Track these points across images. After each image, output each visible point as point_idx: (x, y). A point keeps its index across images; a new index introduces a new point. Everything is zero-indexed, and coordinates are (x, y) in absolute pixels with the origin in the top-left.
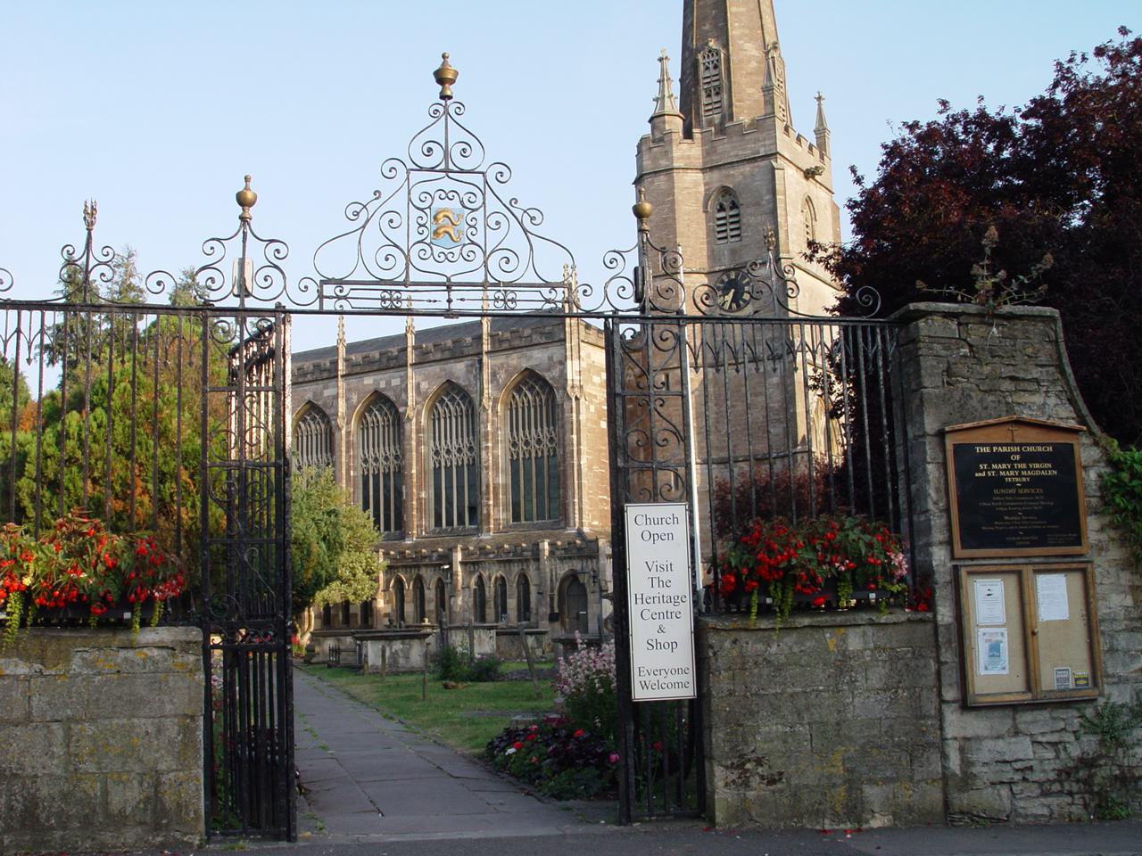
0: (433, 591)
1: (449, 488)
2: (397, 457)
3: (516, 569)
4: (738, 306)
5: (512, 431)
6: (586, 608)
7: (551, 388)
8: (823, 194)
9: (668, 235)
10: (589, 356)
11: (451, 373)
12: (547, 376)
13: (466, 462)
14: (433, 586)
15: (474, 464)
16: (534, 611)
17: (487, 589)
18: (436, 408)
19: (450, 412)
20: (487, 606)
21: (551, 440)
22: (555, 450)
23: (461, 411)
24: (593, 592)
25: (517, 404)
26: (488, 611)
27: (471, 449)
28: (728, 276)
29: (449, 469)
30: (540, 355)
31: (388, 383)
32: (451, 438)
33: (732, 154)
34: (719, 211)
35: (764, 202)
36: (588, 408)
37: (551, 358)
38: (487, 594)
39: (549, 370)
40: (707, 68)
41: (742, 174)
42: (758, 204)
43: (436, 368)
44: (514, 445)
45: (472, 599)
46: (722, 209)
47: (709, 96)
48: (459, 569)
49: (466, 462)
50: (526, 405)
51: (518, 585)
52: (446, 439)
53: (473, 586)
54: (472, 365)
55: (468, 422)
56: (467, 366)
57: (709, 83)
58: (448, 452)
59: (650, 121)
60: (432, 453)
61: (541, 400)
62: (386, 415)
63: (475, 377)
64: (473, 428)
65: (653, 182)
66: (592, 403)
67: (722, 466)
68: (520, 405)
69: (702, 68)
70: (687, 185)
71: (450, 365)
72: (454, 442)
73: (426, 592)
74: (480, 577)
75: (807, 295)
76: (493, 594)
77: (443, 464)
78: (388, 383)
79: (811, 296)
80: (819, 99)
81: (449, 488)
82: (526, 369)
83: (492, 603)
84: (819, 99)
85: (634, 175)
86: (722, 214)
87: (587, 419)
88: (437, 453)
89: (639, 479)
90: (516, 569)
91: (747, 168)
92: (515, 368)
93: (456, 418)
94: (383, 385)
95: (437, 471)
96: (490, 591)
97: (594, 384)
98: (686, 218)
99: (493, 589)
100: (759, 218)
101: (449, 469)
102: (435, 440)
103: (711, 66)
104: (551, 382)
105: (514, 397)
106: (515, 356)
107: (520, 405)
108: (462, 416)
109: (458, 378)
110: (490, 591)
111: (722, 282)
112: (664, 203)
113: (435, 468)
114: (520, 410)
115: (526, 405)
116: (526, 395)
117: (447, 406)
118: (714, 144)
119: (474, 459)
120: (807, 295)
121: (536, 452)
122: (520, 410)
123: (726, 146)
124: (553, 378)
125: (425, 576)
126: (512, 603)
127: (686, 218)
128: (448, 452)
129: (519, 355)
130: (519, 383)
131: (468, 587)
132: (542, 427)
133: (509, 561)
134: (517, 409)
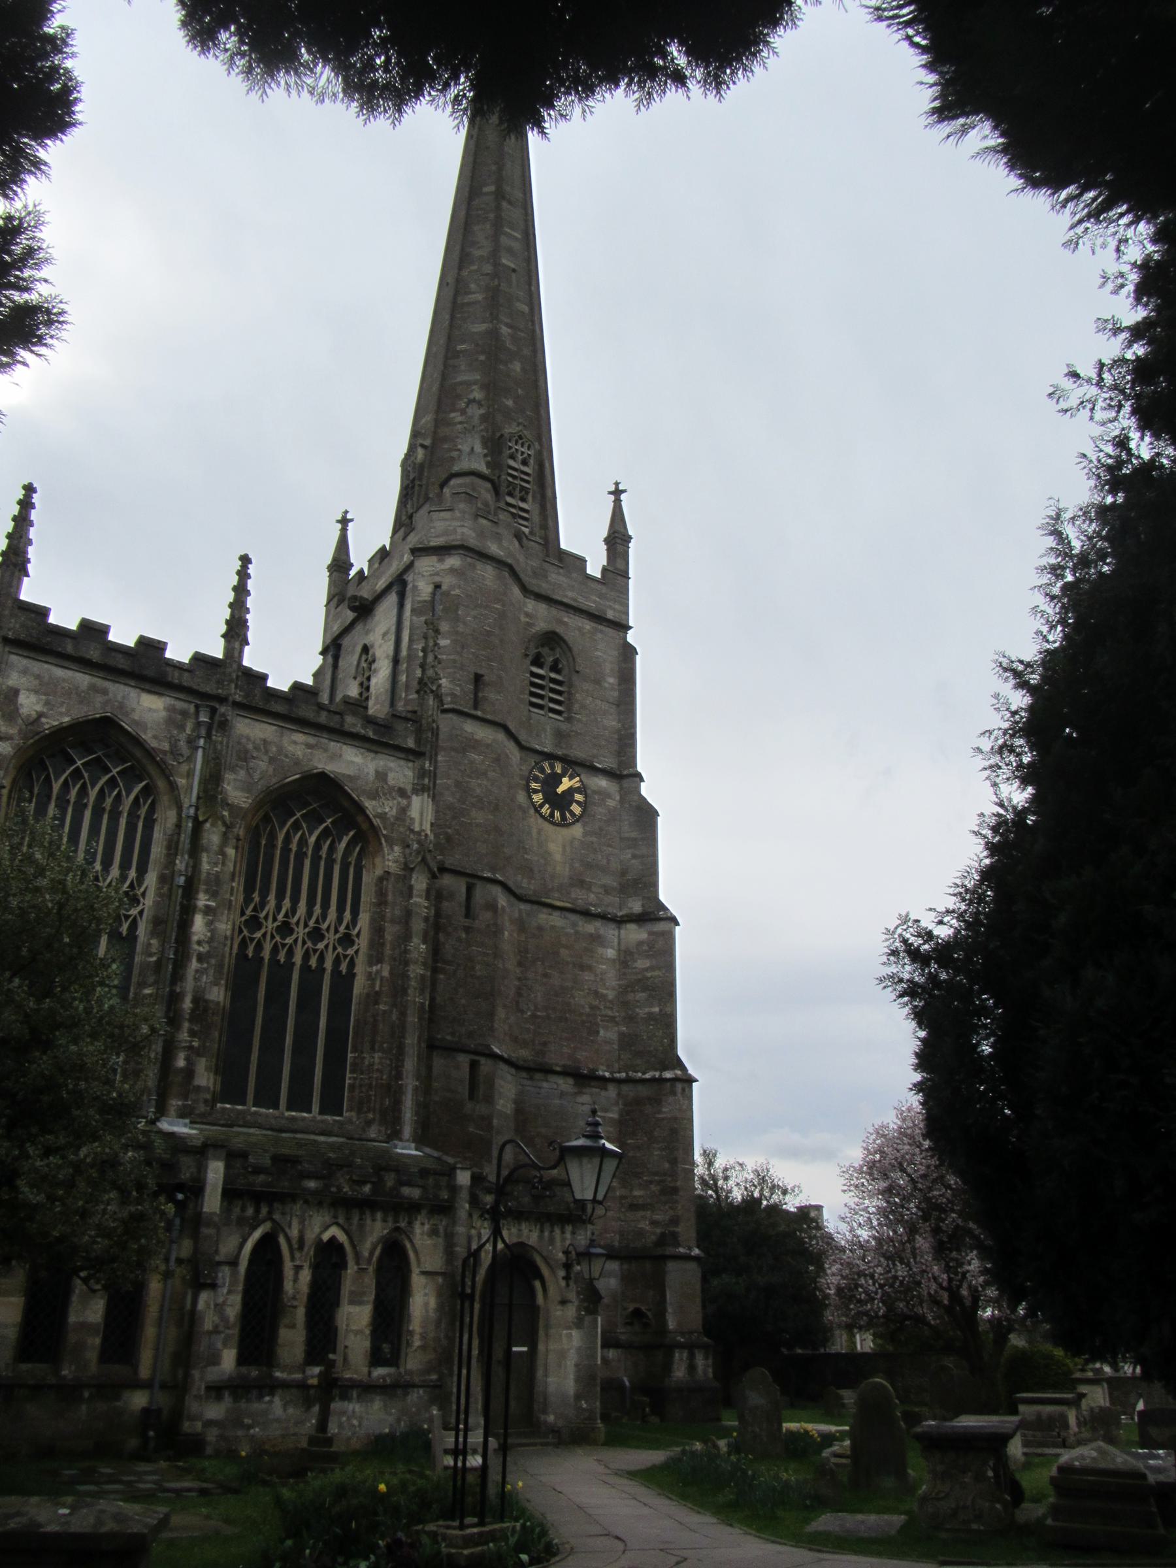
3: (377, 1229)
4: (563, 817)
12: (370, 805)
20: (285, 1321)
24: (564, 1302)
26: (284, 1334)
28: (552, 767)
33: (570, 594)
35: (606, 685)
37: (381, 776)
38: (288, 1286)
39: (374, 795)
40: (512, 457)
41: (580, 629)
42: (598, 682)
43: (83, 680)
45: (237, 1299)
46: (537, 661)
47: (510, 494)
48: (212, 1202)
51: (379, 1270)
54: (184, 713)
56: (170, 709)
57: (514, 477)
67: (524, 1074)
71: (127, 689)
82: (323, 776)
83: (301, 1313)
90: (377, 1229)
91: (588, 625)
92: (297, 763)
99: (306, 1276)
100: (599, 702)
106: (299, 737)
111: (542, 770)
118: (546, 565)
124: (382, 817)
129: (311, 740)
131: (233, 1263)
133: (366, 1205)
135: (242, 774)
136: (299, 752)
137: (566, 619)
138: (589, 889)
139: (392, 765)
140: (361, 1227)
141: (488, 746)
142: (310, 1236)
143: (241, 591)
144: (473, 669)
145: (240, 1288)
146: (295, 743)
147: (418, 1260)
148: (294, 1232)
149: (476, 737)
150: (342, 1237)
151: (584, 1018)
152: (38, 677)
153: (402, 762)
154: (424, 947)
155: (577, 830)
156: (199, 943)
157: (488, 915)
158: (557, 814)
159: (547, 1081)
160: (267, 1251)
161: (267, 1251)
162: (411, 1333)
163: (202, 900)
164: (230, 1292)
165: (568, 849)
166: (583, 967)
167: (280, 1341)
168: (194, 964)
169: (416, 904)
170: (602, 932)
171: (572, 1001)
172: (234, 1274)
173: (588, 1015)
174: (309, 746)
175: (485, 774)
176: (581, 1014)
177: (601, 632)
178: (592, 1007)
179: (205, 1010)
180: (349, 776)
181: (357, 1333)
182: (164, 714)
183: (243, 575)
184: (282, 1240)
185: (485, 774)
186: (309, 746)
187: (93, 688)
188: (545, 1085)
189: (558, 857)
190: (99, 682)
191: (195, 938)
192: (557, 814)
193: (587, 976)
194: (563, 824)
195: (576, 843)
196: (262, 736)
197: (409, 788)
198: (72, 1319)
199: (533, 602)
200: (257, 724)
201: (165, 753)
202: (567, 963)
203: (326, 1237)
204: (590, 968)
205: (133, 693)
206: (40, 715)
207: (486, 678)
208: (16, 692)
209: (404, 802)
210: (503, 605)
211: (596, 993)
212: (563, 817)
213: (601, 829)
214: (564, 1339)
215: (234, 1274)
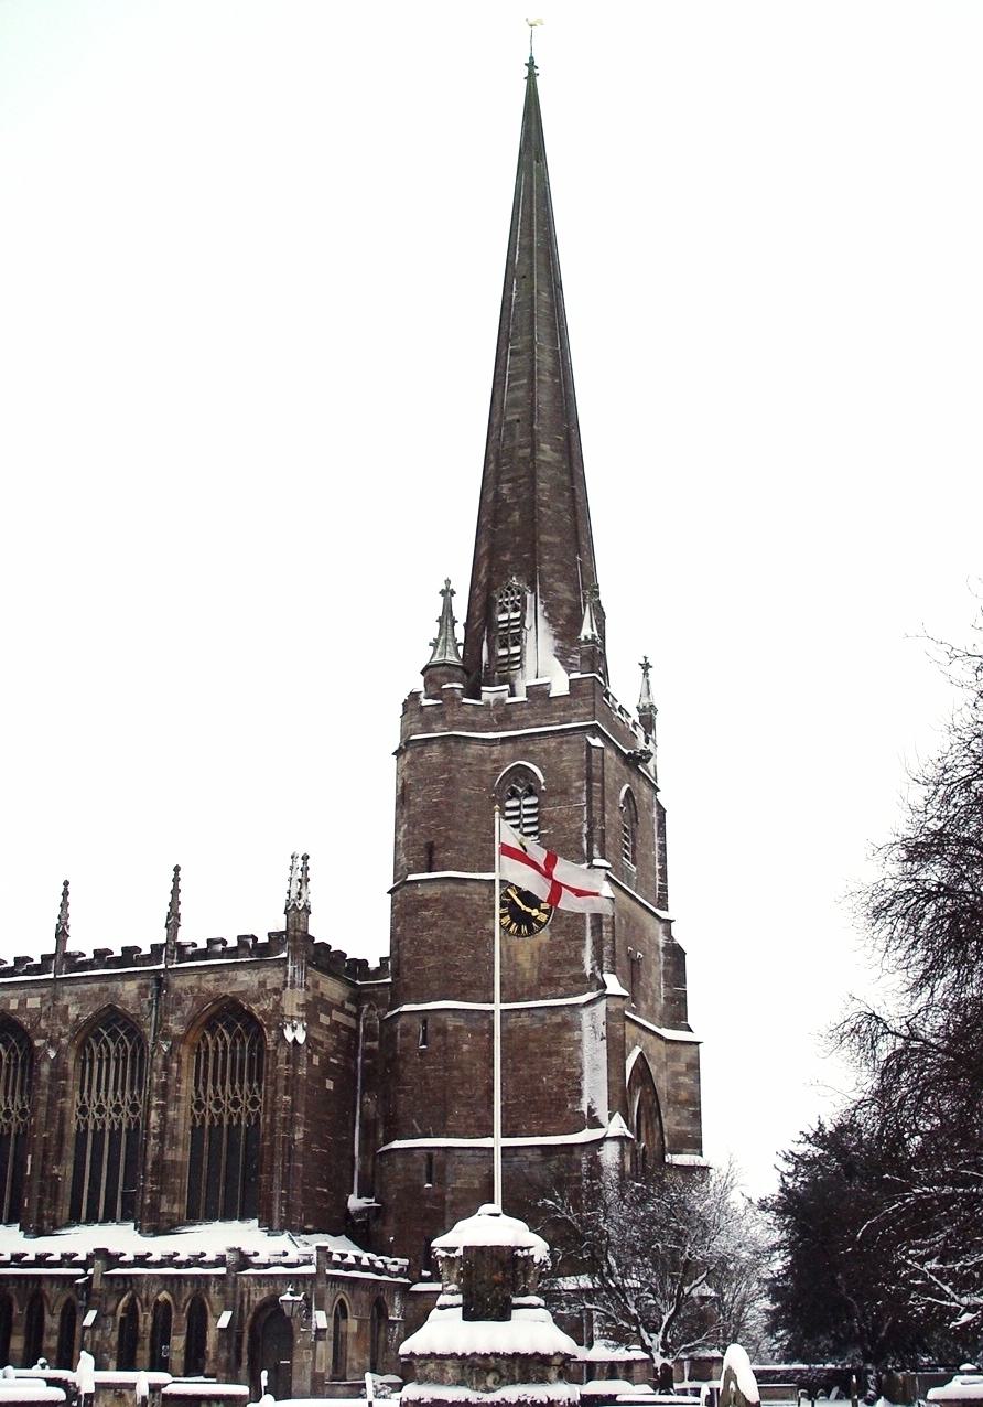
0: (57, 1319)
1: (96, 1163)
2: (23, 1113)
5: (196, 1085)
6: (291, 1359)
7: (259, 1025)
8: (646, 790)
9: (438, 826)
10: (316, 985)
11: (116, 996)
13: (125, 1126)
14: (58, 1311)
15: (137, 1129)
16: (211, 1357)
17: (141, 1319)
18: (89, 1045)
19: (109, 1052)
20: (139, 1346)
21: (254, 1103)
22: (258, 1118)
23: (125, 1051)
25: (207, 1047)
27: (134, 1108)
29: (98, 1136)
30: (246, 979)
31: (23, 1003)
32: (106, 1090)
34: (510, 798)
35: (573, 791)
36: (310, 1059)
37: (262, 984)
38: (141, 1326)
39: (257, 1000)
40: (504, 611)
41: (545, 750)
44: (199, 1105)
45: (116, 1334)
49: (125, 1126)
50: (221, 1048)
51: (189, 1318)
52: (98, 1090)
53: (120, 1314)
54: (147, 987)
55: (133, 1072)
56: (140, 987)
58: (100, 1110)
59: (423, 673)
60: (76, 1109)
61: (243, 1043)
62: (14, 1049)
63: (150, 1002)
64: (141, 1077)
65: (422, 753)
66: (315, 1052)
68: (211, 1048)
69: (498, 609)
70: (469, 761)
71: (115, 983)
72: (110, 1095)
73: (47, 1318)
74: (132, 1300)
75: (623, 922)
76: (149, 1328)
77: (91, 1126)
78: (23, 1003)
79: (627, 924)
80: (646, 666)
81: (96, 1163)
82: (226, 996)
83: (147, 1340)
84: (646, 666)
85: (396, 743)
86: (514, 803)
87: (309, 1075)
88: (83, 1110)
89: (374, 1165)
92: (210, 994)
93: (117, 1060)
94: (14, 1005)
95: (81, 1137)
96: (146, 1320)
97: (321, 1025)
98: (465, 804)
99: (150, 1320)
101: (98, 1136)
102: (82, 1092)
103: (509, 607)
104: (260, 1017)
105: (204, 1036)
107: (211, 1048)
108: (125, 1059)
109: (125, 1003)
110: (146, 1320)
112: (436, 781)
113: (78, 1132)
114: (211, 1055)
115: (221, 1048)
116: (222, 1035)
117: (105, 1042)
119: (137, 1124)
120: (623, 922)
121: (230, 1119)
122: (211, 1055)
123: (525, 712)
124: (263, 1013)
125: (47, 1293)
126: (178, 1342)
127: (465, 804)
128: (100, 1110)
129: (218, 976)
130: (213, 1016)
131: (114, 1314)
132: (241, 1083)
134: (206, 1054)
135: (179, 1014)
136: (210, 986)
137: (531, 748)
138: (558, 984)
139: (269, 973)
140: (179, 1290)
141: (437, 900)
142: (151, 1297)
143: (175, 891)
144: (424, 841)
145: (117, 1328)
146: (208, 981)
147: (212, 1309)
148: (144, 1296)
149: (426, 897)
150: (169, 1298)
151: (553, 1097)
152: (76, 994)
153: (276, 969)
154: (288, 1098)
155: (544, 935)
156: (154, 1128)
157: (439, 1038)
158: (524, 929)
159: (516, 1155)
160: (131, 1311)
161: (131, 1311)
162: (208, 1352)
163: (155, 1102)
164: (113, 1330)
165: (536, 955)
166: (550, 1054)
167: (138, 1357)
168: (152, 1141)
169: (280, 1069)
170: (569, 1018)
171: (540, 1085)
172: (115, 1320)
173: (556, 1093)
174: (216, 980)
175: (435, 924)
176: (549, 1094)
177: (568, 742)
178: (562, 1086)
179: (164, 1167)
180: (241, 992)
181: (176, 1351)
182: (136, 991)
183: (176, 880)
184: (137, 1301)
185: (435, 924)
186: (216, 980)
187: (102, 990)
188: (515, 1159)
189: (527, 965)
190: (103, 984)
191: (152, 1126)
192: (524, 929)
193: (555, 1061)
194: (531, 931)
195: (544, 948)
196: (189, 984)
197: (280, 987)
198: (44, 1346)
199: (499, 747)
200: (186, 978)
201: (138, 1015)
202: (536, 1053)
203: (160, 1298)
204: (557, 1053)
205: (120, 984)
206: (78, 1016)
207: (436, 843)
208: (67, 1007)
209: (277, 997)
210: (450, 773)
211: (564, 1073)
212: (519, 930)
213: (568, 926)
214: (304, 1356)
215: (115, 1320)
